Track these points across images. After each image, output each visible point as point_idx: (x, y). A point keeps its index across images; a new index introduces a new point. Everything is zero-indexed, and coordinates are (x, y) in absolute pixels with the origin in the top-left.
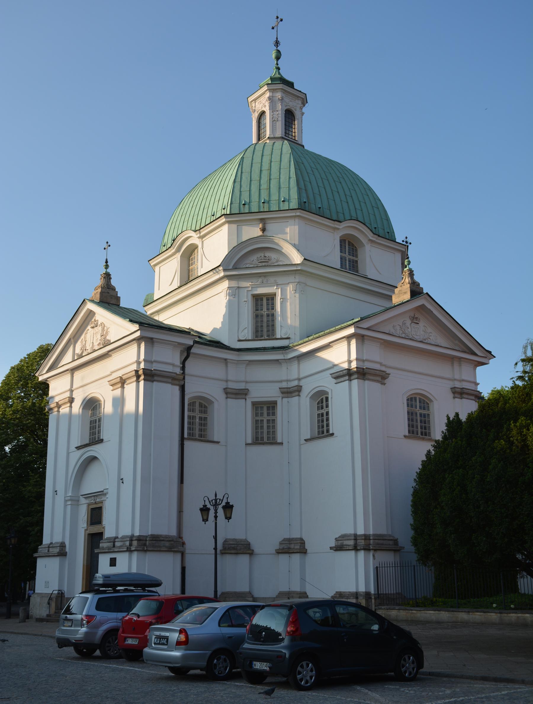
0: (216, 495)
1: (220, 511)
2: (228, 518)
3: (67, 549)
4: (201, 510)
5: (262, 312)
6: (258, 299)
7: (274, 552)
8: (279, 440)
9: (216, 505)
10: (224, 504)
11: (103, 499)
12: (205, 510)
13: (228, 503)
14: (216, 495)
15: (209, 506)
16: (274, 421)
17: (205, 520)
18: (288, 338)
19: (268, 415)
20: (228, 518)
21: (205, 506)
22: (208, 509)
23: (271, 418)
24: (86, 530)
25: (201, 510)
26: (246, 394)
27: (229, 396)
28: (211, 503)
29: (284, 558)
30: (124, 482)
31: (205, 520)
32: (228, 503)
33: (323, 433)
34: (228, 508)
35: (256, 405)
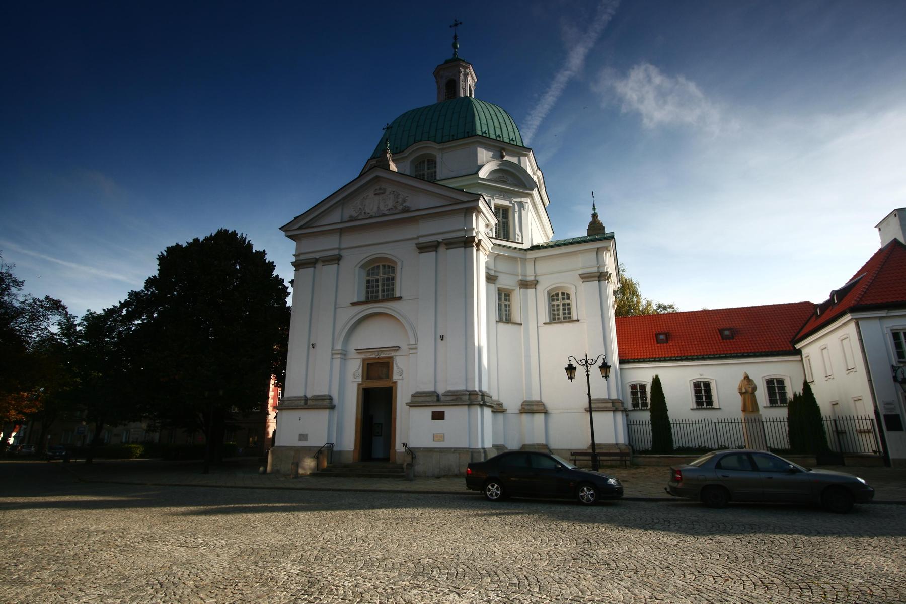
0: (586, 357)
1: (595, 371)
3: (336, 401)
4: (566, 369)
5: (503, 220)
7: (518, 412)
10: (600, 363)
11: (392, 355)
12: (570, 369)
14: (586, 357)
16: (509, 305)
17: (571, 378)
18: (522, 243)
19: (506, 300)
22: (575, 368)
23: (507, 303)
24: (359, 384)
25: (566, 369)
26: (495, 280)
28: (581, 364)
29: (525, 417)
30: (444, 338)
31: (571, 378)
33: (559, 319)
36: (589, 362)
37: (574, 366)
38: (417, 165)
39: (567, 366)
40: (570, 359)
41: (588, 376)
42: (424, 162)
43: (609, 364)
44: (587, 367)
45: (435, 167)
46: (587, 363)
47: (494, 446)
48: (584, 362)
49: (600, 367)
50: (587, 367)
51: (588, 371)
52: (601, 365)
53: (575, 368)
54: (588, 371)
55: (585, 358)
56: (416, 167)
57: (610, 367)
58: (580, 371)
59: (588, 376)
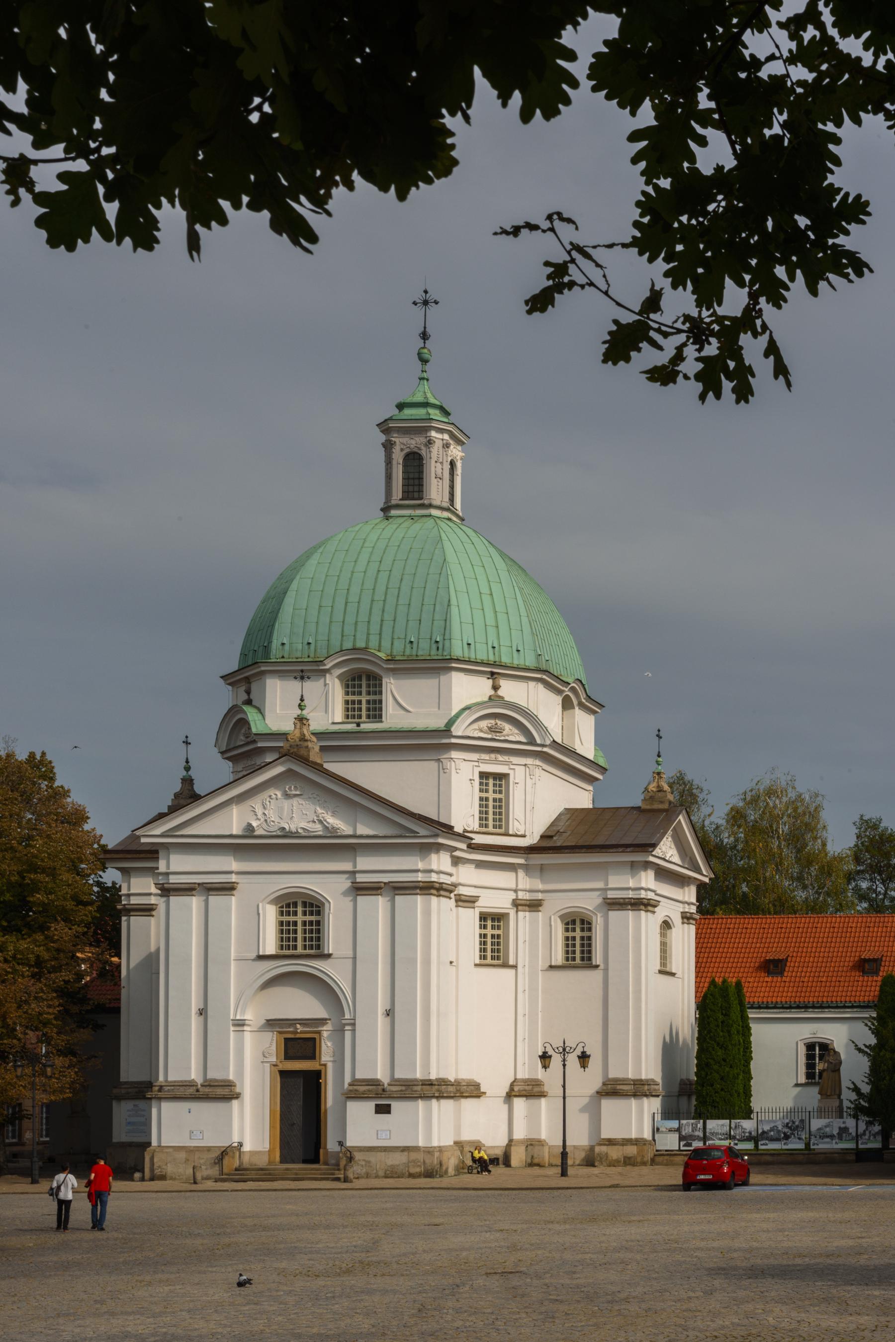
0: (564, 1043)
1: (573, 1060)
2: (584, 1066)
4: (540, 1057)
6: (484, 775)
8: (511, 962)
9: (564, 1051)
12: (545, 1058)
13: (583, 1053)
14: (564, 1043)
15: (550, 1052)
17: (545, 1067)
20: (584, 1066)
21: (545, 1053)
22: (550, 1057)
27: (460, 904)
32: (583, 1053)
34: (584, 1058)
35: (483, 917)
36: (568, 1049)
37: (550, 1053)
38: (348, 681)
39: (540, 1054)
40: (545, 1045)
41: (564, 1065)
42: (360, 678)
43: (588, 1053)
44: (564, 1055)
45: (381, 693)
46: (564, 1051)
47: (455, 1143)
48: (561, 1050)
49: (579, 1057)
50: (564, 1055)
51: (564, 1060)
52: (579, 1054)
53: (550, 1057)
54: (564, 1060)
55: (562, 1045)
56: (347, 686)
57: (589, 1056)
58: (556, 1060)
59: (564, 1065)
